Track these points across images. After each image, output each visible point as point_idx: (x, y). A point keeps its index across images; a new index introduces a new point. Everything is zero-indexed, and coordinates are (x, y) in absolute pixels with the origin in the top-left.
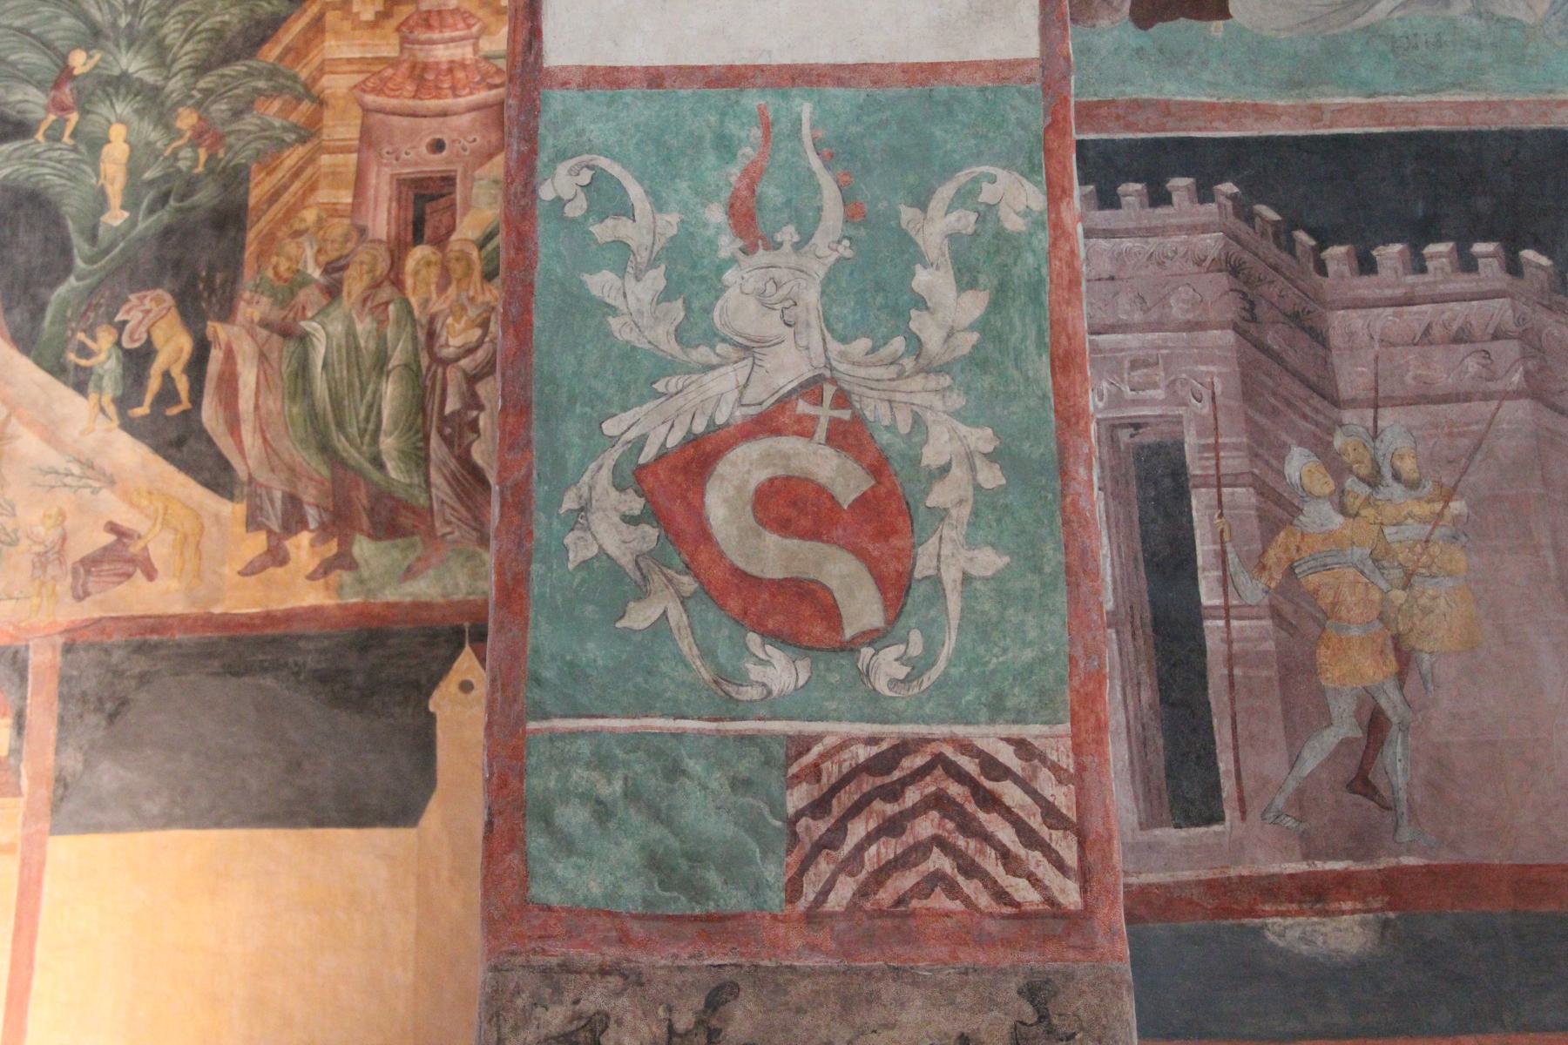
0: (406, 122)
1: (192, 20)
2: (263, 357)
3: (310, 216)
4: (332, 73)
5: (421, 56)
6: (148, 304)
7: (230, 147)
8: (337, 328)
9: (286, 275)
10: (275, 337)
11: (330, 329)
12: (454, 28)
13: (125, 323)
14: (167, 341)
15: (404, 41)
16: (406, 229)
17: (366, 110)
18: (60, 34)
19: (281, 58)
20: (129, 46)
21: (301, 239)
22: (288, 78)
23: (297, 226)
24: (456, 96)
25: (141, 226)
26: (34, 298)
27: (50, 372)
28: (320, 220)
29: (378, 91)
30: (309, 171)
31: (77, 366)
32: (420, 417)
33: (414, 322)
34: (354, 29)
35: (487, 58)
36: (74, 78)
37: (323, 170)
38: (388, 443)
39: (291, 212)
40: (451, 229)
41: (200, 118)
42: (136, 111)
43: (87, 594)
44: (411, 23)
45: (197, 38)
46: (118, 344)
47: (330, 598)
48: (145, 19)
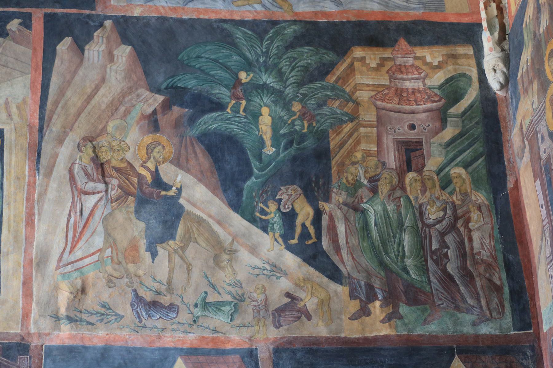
0: (396, 115)
1: (294, 61)
2: (346, 219)
3: (359, 155)
4: (360, 90)
5: (399, 85)
6: (290, 192)
7: (318, 121)
8: (379, 208)
9: (352, 182)
10: (351, 210)
11: (375, 208)
12: (413, 73)
13: (280, 200)
14: (301, 209)
15: (391, 78)
16: (403, 164)
17: (378, 108)
18: (233, 63)
19: (337, 81)
20: (266, 71)
21: (356, 166)
22: (341, 91)
23: (354, 159)
24: (417, 105)
25: (282, 155)
26: (237, 186)
27: (249, 221)
28: (363, 158)
29: (383, 101)
30: (355, 135)
31: (261, 219)
32: (422, 251)
33: (412, 206)
34: (368, 71)
35: (430, 88)
36: (242, 84)
37: (362, 134)
38: (409, 262)
39: (350, 153)
40: (424, 165)
41: (303, 107)
42: (273, 102)
43: (280, 326)
44: (393, 70)
45: (297, 70)
46: (279, 209)
47: (392, 332)
48: (272, 59)
